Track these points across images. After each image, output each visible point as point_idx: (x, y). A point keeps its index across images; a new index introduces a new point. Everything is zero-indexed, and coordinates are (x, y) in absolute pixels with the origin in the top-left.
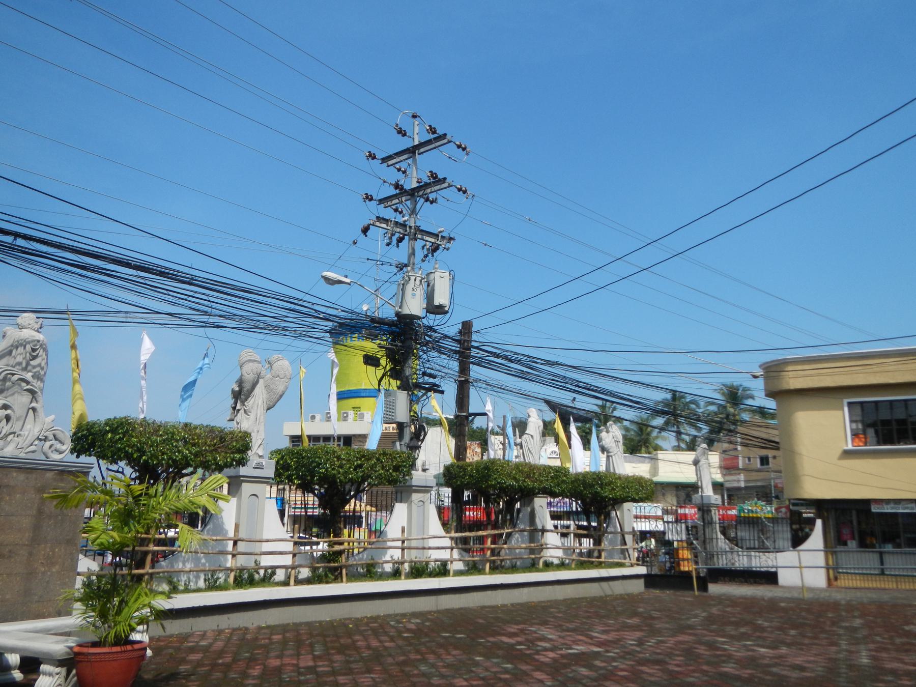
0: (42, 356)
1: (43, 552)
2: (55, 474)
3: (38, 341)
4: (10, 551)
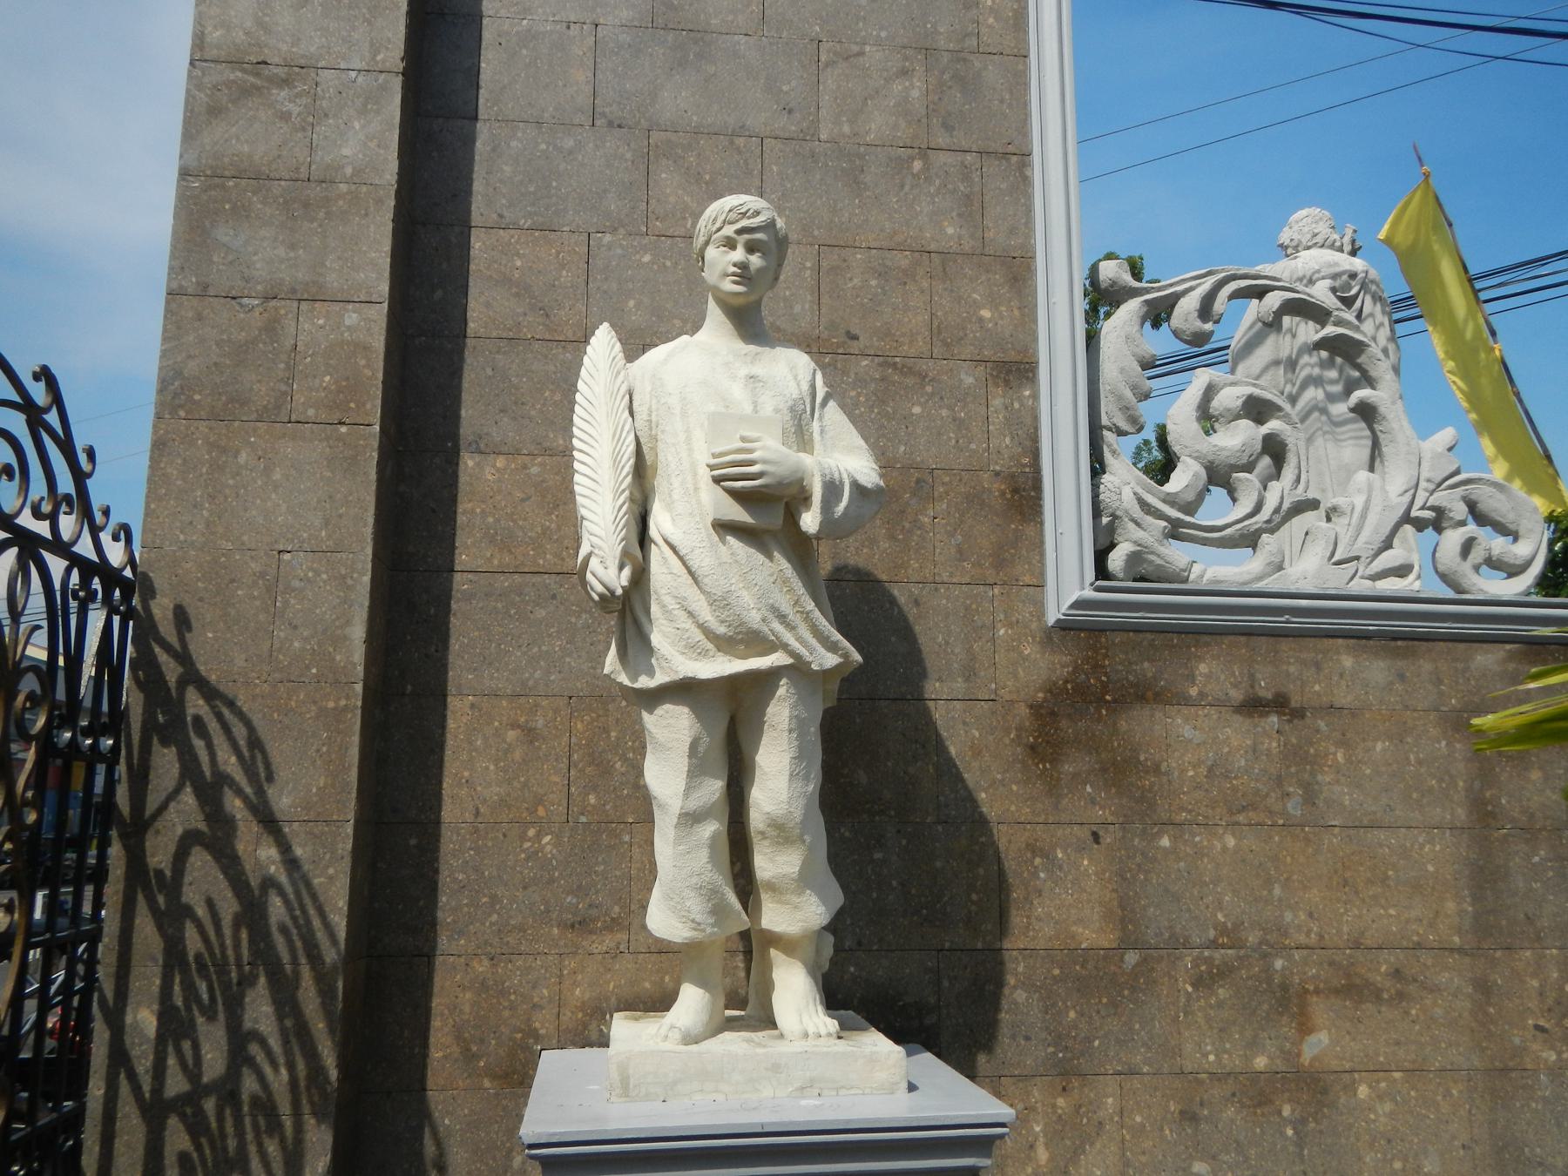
0: (1371, 315)
1: (1535, 983)
2: (1511, 657)
3: (1353, 276)
4: (1397, 974)
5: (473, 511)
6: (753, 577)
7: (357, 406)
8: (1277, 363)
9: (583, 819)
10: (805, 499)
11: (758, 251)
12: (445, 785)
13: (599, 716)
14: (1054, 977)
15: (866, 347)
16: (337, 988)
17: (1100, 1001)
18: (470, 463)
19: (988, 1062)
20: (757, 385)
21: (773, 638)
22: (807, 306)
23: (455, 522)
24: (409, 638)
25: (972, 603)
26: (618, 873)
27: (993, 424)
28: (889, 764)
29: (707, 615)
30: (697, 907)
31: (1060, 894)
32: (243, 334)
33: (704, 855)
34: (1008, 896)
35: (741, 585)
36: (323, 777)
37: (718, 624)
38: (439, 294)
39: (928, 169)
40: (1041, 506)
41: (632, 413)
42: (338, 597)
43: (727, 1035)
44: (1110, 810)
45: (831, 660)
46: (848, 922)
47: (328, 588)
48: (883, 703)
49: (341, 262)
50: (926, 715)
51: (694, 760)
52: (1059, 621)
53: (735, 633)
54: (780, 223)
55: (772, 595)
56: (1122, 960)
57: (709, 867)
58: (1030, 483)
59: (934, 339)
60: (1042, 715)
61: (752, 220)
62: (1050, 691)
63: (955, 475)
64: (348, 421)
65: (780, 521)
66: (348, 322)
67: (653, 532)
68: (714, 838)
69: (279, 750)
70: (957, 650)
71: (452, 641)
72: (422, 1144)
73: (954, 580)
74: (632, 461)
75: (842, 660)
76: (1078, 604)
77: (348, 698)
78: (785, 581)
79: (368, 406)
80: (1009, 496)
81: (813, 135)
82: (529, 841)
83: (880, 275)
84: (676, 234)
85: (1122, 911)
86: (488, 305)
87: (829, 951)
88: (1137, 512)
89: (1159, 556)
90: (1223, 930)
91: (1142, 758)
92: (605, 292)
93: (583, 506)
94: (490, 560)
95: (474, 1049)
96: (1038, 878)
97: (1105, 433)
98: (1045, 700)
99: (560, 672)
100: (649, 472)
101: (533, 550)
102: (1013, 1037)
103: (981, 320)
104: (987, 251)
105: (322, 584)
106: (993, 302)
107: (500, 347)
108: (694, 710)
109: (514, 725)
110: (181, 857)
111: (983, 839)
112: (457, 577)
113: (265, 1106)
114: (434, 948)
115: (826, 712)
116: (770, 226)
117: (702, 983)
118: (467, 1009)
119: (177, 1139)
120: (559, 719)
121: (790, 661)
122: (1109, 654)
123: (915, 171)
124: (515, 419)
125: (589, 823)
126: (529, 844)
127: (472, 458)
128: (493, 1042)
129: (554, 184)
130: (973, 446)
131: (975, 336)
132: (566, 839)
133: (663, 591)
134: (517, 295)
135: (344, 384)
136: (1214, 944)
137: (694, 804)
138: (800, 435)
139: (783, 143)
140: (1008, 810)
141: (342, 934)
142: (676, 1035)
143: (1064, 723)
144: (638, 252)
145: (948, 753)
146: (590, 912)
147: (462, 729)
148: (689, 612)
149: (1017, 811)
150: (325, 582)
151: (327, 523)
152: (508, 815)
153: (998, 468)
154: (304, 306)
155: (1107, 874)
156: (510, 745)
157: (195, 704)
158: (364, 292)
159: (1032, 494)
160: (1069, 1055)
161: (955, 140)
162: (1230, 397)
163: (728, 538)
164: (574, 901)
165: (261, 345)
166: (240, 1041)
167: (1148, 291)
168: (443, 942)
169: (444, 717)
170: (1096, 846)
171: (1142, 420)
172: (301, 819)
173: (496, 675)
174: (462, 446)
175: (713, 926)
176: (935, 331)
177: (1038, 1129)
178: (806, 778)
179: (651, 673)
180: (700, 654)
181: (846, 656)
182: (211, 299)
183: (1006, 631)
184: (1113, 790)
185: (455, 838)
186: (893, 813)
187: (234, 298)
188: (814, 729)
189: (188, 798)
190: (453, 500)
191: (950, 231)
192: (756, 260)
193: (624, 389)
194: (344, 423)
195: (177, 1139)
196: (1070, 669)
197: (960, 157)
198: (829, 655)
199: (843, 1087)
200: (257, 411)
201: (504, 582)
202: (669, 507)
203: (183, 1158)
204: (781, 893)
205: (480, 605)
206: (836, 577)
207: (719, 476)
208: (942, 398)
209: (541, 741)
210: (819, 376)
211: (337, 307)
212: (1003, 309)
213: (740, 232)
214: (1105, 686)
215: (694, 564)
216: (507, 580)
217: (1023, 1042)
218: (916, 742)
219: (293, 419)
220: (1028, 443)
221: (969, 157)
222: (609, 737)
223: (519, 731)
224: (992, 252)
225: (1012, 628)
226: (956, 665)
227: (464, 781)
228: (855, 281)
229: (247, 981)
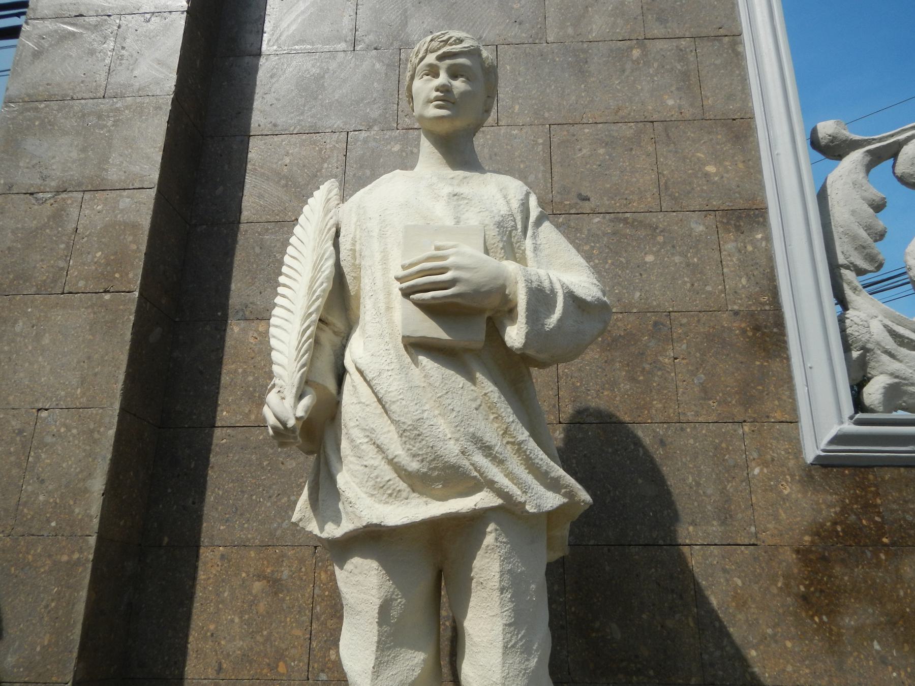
5: (236, 371)
6: (449, 401)
7: (121, 276)
9: (323, 677)
10: (510, 313)
11: (462, 76)
12: (191, 639)
15: (598, 206)
20: (461, 202)
21: (476, 474)
22: (540, 175)
23: (219, 380)
25: (721, 442)
28: (644, 616)
29: (397, 449)
32: (35, 222)
35: (437, 412)
36: (48, 635)
39: (646, 55)
40: (785, 342)
41: (336, 245)
42: (85, 450)
44: (906, 671)
45: (552, 500)
47: (76, 442)
48: (634, 550)
49: (121, 159)
50: (682, 561)
51: (386, 628)
52: (818, 458)
53: (430, 469)
55: (474, 423)
58: (771, 320)
59: (662, 195)
60: (811, 560)
61: (454, 46)
63: (693, 316)
65: (482, 336)
66: (122, 205)
67: (348, 363)
70: (709, 492)
71: (208, 493)
73: (700, 419)
75: (566, 500)
76: (839, 439)
77: (81, 551)
78: (492, 407)
79: (131, 275)
80: (750, 334)
81: (541, 39)
83: (607, 144)
88: (890, 344)
93: (274, 337)
94: (247, 415)
97: (843, 271)
100: (353, 303)
103: (707, 175)
104: (707, 116)
105: (71, 439)
107: (267, 229)
109: (260, 576)
112: (218, 432)
115: (549, 566)
116: (473, 53)
120: (303, 569)
121: (497, 502)
122: (880, 491)
123: (634, 58)
127: (237, 325)
130: (709, 288)
131: (702, 190)
133: (352, 424)
135: (112, 258)
138: (512, 251)
139: (515, 48)
140: (784, 670)
143: (838, 570)
144: (390, 143)
145: (710, 604)
147: (211, 580)
148: (378, 446)
149: (794, 671)
151: (83, 381)
152: (249, 671)
153: (736, 307)
154: (87, 196)
156: (255, 596)
158: (137, 180)
159: (775, 330)
161: (669, 30)
163: (421, 358)
165: (48, 231)
167: (868, 142)
169: (196, 568)
171: (881, 257)
172: (22, 680)
173: (246, 525)
174: (231, 312)
176: (662, 188)
178: (527, 651)
179: (337, 521)
180: (390, 495)
181: (570, 494)
182: (13, 196)
183: (761, 470)
186: (651, 673)
187: (32, 194)
188: (537, 589)
190: (220, 362)
191: (671, 102)
192: (459, 85)
193: (332, 222)
194: (108, 292)
196: (838, 509)
197: (675, 43)
198: (550, 494)
200: (37, 286)
205: (236, 458)
206: (577, 420)
207: (408, 287)
208: (674, 247)
209: (285, 592)
210: (533, 201)
211: (113, 194)
212: (727, 163)
213: (441, 58)
214: (880, 527)
216: (262, 434)
218: (673, 591)
219: (65, 292)
220: (765, 282)
221: (683, 43)
223: (265, 581)
224: (712, 117)
225: (767, 467)
226: (709, 507)
227: (209, 634)
228: (584, 151)
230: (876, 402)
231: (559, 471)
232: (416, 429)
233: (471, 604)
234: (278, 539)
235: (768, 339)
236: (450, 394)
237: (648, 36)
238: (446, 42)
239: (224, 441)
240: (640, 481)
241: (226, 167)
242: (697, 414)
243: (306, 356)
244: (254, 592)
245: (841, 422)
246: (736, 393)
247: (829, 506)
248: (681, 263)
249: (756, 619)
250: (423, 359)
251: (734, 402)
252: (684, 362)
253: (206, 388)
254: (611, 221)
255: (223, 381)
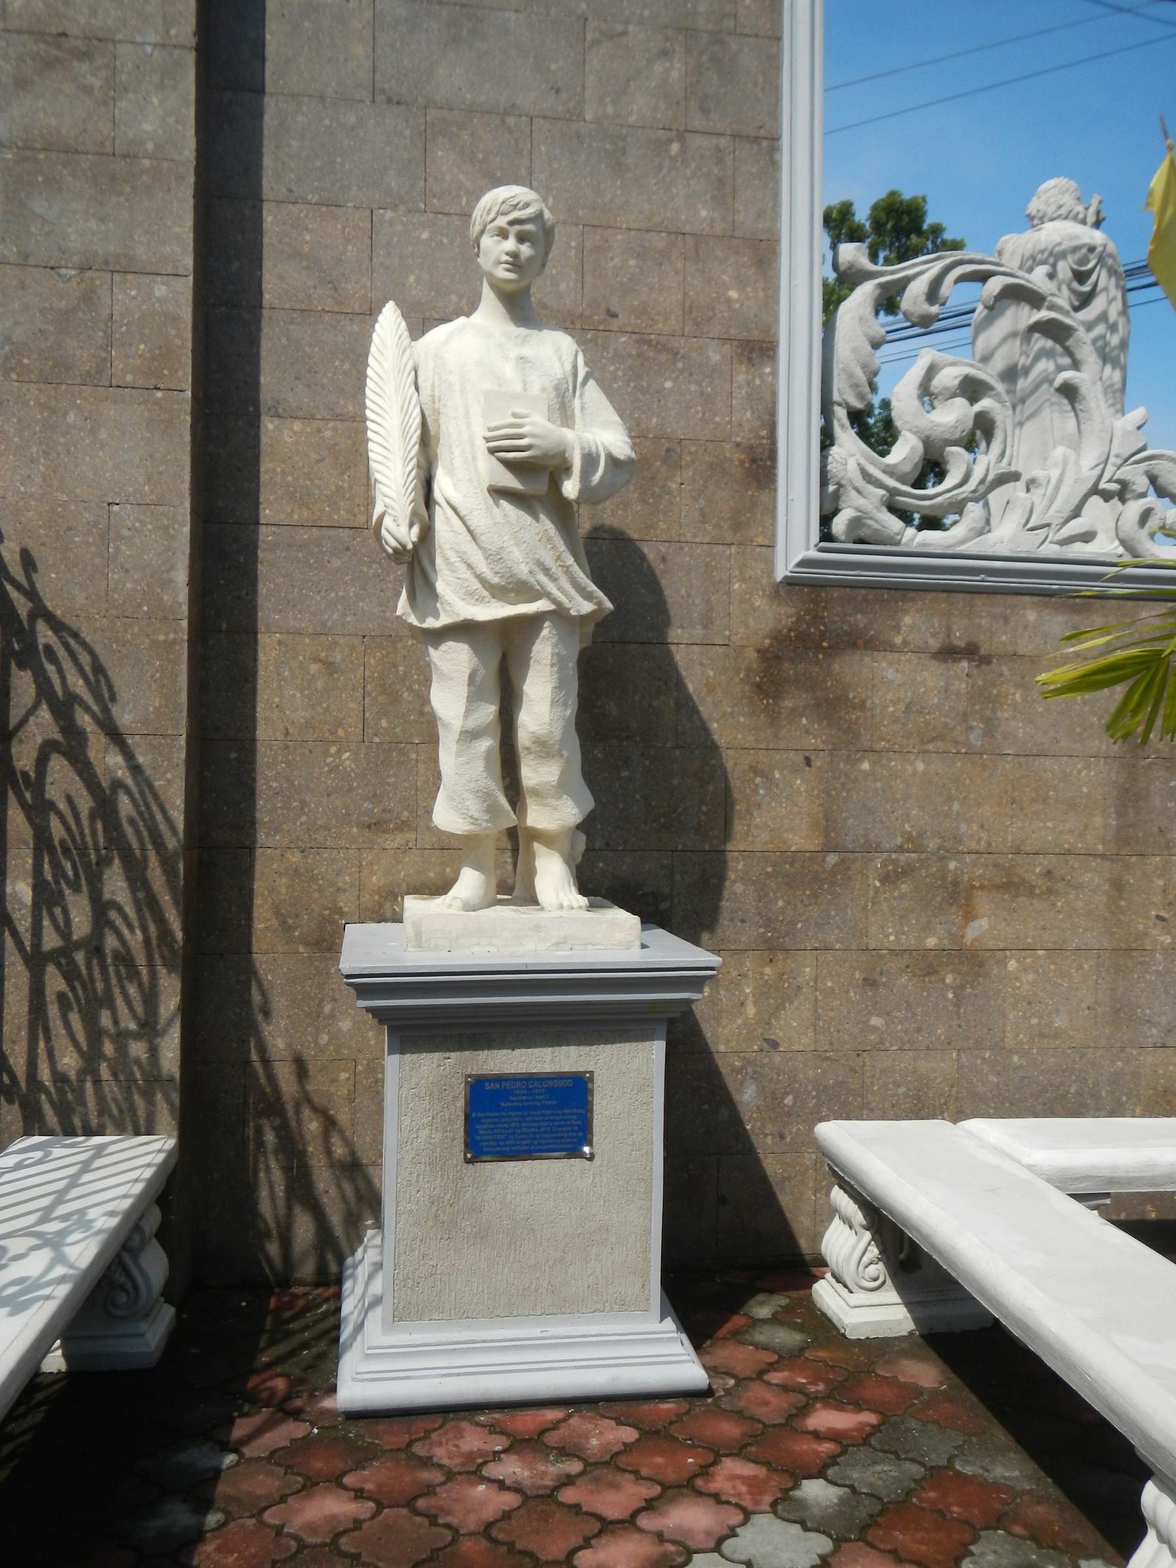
0: (1106, 289)
1: (1161, 883)
3: (1092, 249)
4: (1049, 874)
5: (274, 470)
6: (522, 535)
8: (1014, 334)
9: (376, 740)
10: (567, 470)
11: (528, 241)
12: (258, 709)
13: (388, 653)
14: (768, 874)
15: (624, 325)
16: (179, 869)
17: (804, 893)
18: (270, 426)
19: (710, 939)
22: (571, 284)
23: (259, 479)
24: (222, 582)
26: (406, 784)
27: (736, 398)
28: (636, 698)
29: (483, 568)
30: (474, 807)
31: (775, 807)
32: (64, 303)
33: (480, 765)
34: (732, 808)
35: (512, 542)
36: (158, 699)
37: (492, 575)
38: (235, 266)
43: (498, 907)
45: (587, 607)
46: (599, 827)
47: (153, 536)
48: (632, 646)
49: (148, 237)
51: (472, 688)
52: (786, 577)
54: (547, 214)
56: (824, 861)
57: (485, 774)
58: (767, 453)
59: (686, 318)
61: (522, 212)
62: (775, 638)
63: (700, 445)
64: (162, 386)
66: (157, 294)
67: (437, 494)
68: (489, 751)
69: (119, 675)
70: (697, 602)
71: (260, 586)
72: (250, 994)
73: (697, 540)
74: (419, 432)
75: (595, 607)
76: (804, 563)
77: (175, 632)
78: (549, 540)
79: (180, 373)
80: (747, 465)
81: (578, 116)
82: (332, 756)
83: (638, 255)
84: (452, 211)
85: (827, 821)
86: (281, 278)
87: (581, 846)
88: (859, 481)
89: (876, 521)
90: (909, 838)
91: (851, 696)
92: (388, 267)
95: (290, 921)
96: (758, 794)
98: (771, 645)
99: (354, 615)
100: (433, 443)
101: (329, 506)
102: (732, 920)
103: (729, 301)
105: (148, 533)
106: (740, 282)
108: (472, 646)
109: (316, 660)
110: (42, 761)
111: (713, 762)
112: (263, 530)
113: (125, 959)
114: (254, 842)
116: (538, 218)
117: (478, 867)
118: (283, 890)
119: (55, 982)
121: (552, 607)
122: (829, 607)
124: (308, 386)
125: (382, 743)
126: (332, 759)
127: (272, 422)
128: (306, 917)
129: (338, 160)
130: (717, 419)
132: (362, 756)
133: (447, 546)
134: (308, 268)
136: (900, 849)
137: (472, 724)
138: (563, 412)
140: (735, 737)
141: (180, 826)
142: (459, 904)
143: (786, 665)
145: (686, 689)
146: (384, 815)
148: (468, 565)
150: (150, 531)
151: (149, 479)
153: (738, 439)
154: (117, 277)
155: (816, 792)
156: (313, 676)
157: (45, 635)
159: (769, 463)
160: (776, 935)
162: (948, 377)
163: (502, 502)
164: (370, 806)
165: (80, 314)
166: (101, 909)
167: (882, 274)
168: (262, 837)
169: (256, 651)
170: (807, 769)
172: (142, 732)
174: (263, 409)
175: (487, 821)
177: (748, 991)
178: (565, 705)
179: (436, 615)
180: (477, 600)
181: (599, 604)
182: (32, 269)
183: (740, 585)
184: (825, 723)
185: (269, 753)
186: (638, 739)
187: (52, 268)
188: (572, 665)
189: (44, 714)
190: (256, 460)
191: (704, 213)
192: (525, 250)
193: (410, 365)
194: (159, 389)
195: (55, 982)
196: (794, 619)
197: (714, 140)
198: (586, 603)
199: (590, 944)
200: (81, 376)
201: (304, 535)
202: (451, 473)
203: (61, 996)
204: (543, 797)
205: (283, 555)
206: (594, 535)
211: (146, 279)
213: (512, 223)
214: (823, 634)
215: (473, 523)
216: (306, 533)
217: (739, 924)
218: (660, 679)
219: (114, 383)
220: (766, 417)
221: (723, 142)
222: (397, 670)
224: (740, 235)
229: (104, 862)
230: (841, 532)
231: (592, 587)
232: (498, 554)
233: (529, 675)
234: (329, 629)
235: (761, 471)
236: (522, 531)
237: (690, 127)
238: (515, 207)
239: (270, 538)
240: (643, 591)
241: (240, 238)
242: (695, 536)
243: (413, 494)
244: (312, 672)
245: (808, 549)
246: (729, 518)
247: (788, 617)
248: (696, 392)
249: (721, 701)
250: (503, 502)
251: (726, 527)
252: (689, 487)
253: (246, 485)
254: (637, 342)
255: (262, 480)
